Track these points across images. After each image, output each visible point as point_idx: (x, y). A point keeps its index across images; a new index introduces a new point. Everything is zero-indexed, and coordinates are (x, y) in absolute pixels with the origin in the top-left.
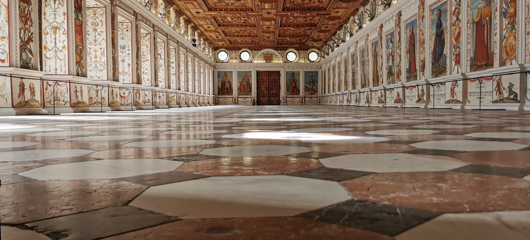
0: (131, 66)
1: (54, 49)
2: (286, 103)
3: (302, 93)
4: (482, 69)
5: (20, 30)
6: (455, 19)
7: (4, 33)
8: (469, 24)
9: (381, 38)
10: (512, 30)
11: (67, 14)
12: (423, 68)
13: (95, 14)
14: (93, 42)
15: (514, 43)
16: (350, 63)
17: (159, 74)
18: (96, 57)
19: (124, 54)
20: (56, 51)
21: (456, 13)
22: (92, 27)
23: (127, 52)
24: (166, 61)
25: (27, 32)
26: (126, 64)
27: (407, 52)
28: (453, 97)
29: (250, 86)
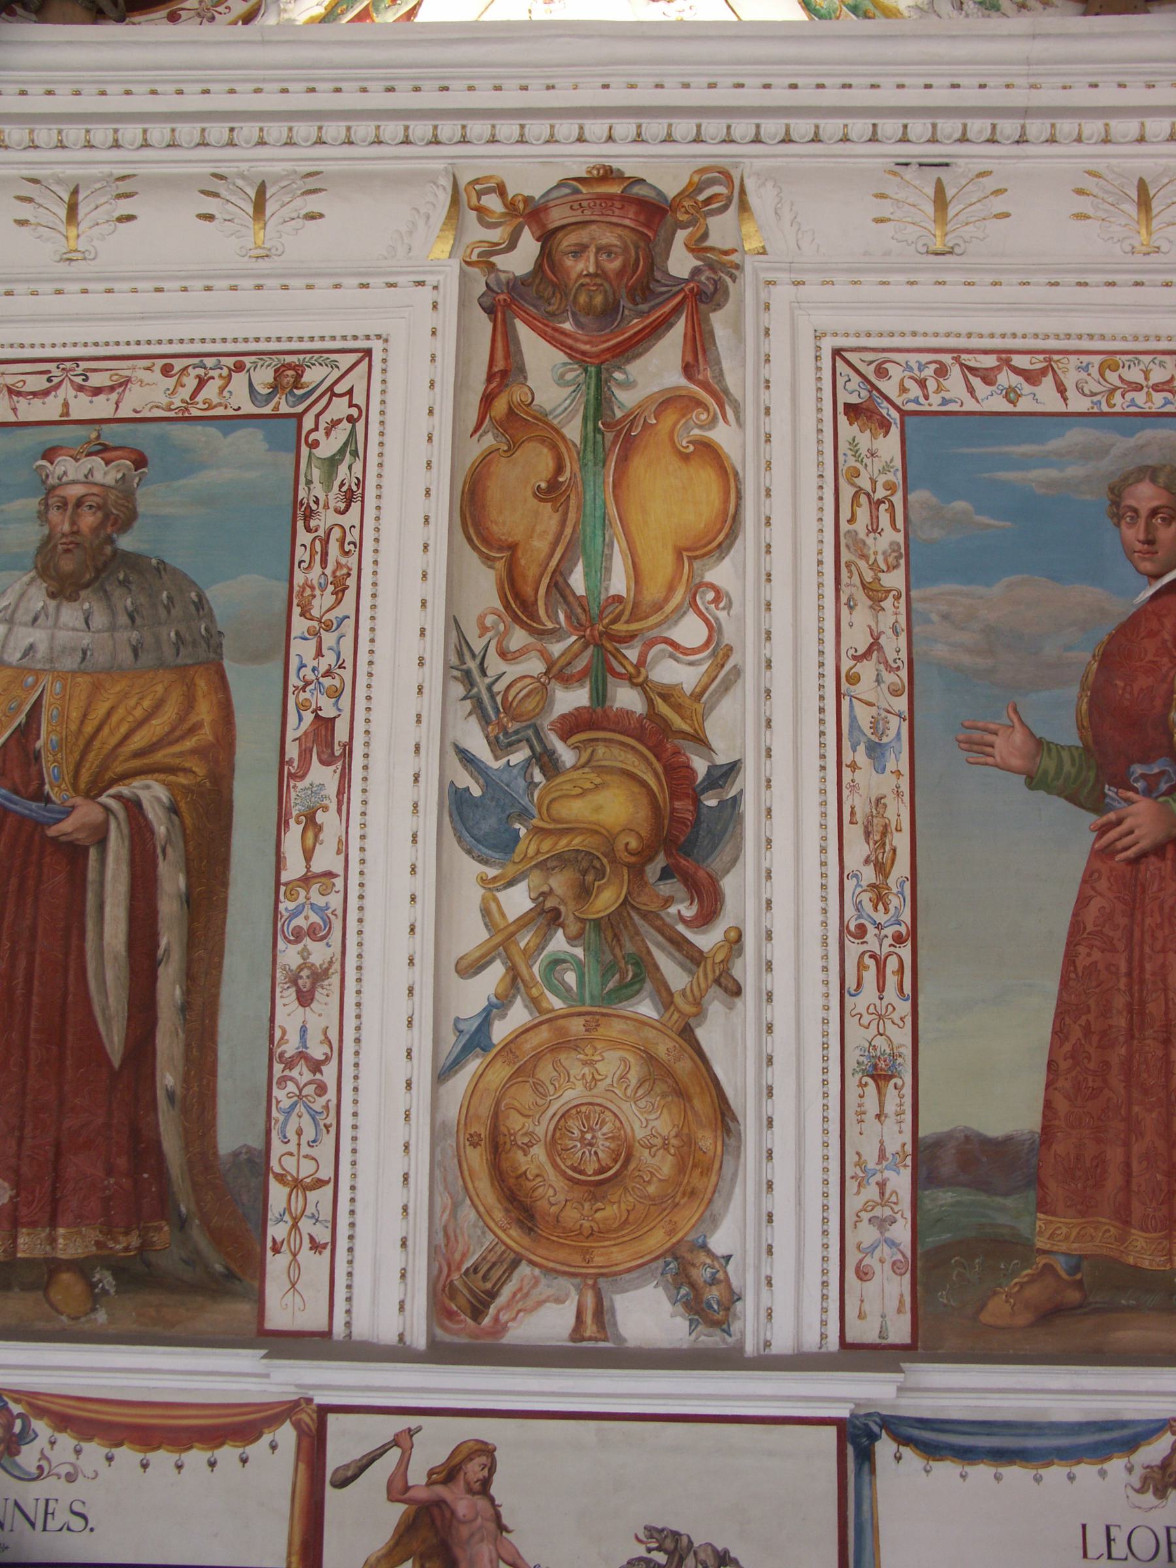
10: (627, 990)
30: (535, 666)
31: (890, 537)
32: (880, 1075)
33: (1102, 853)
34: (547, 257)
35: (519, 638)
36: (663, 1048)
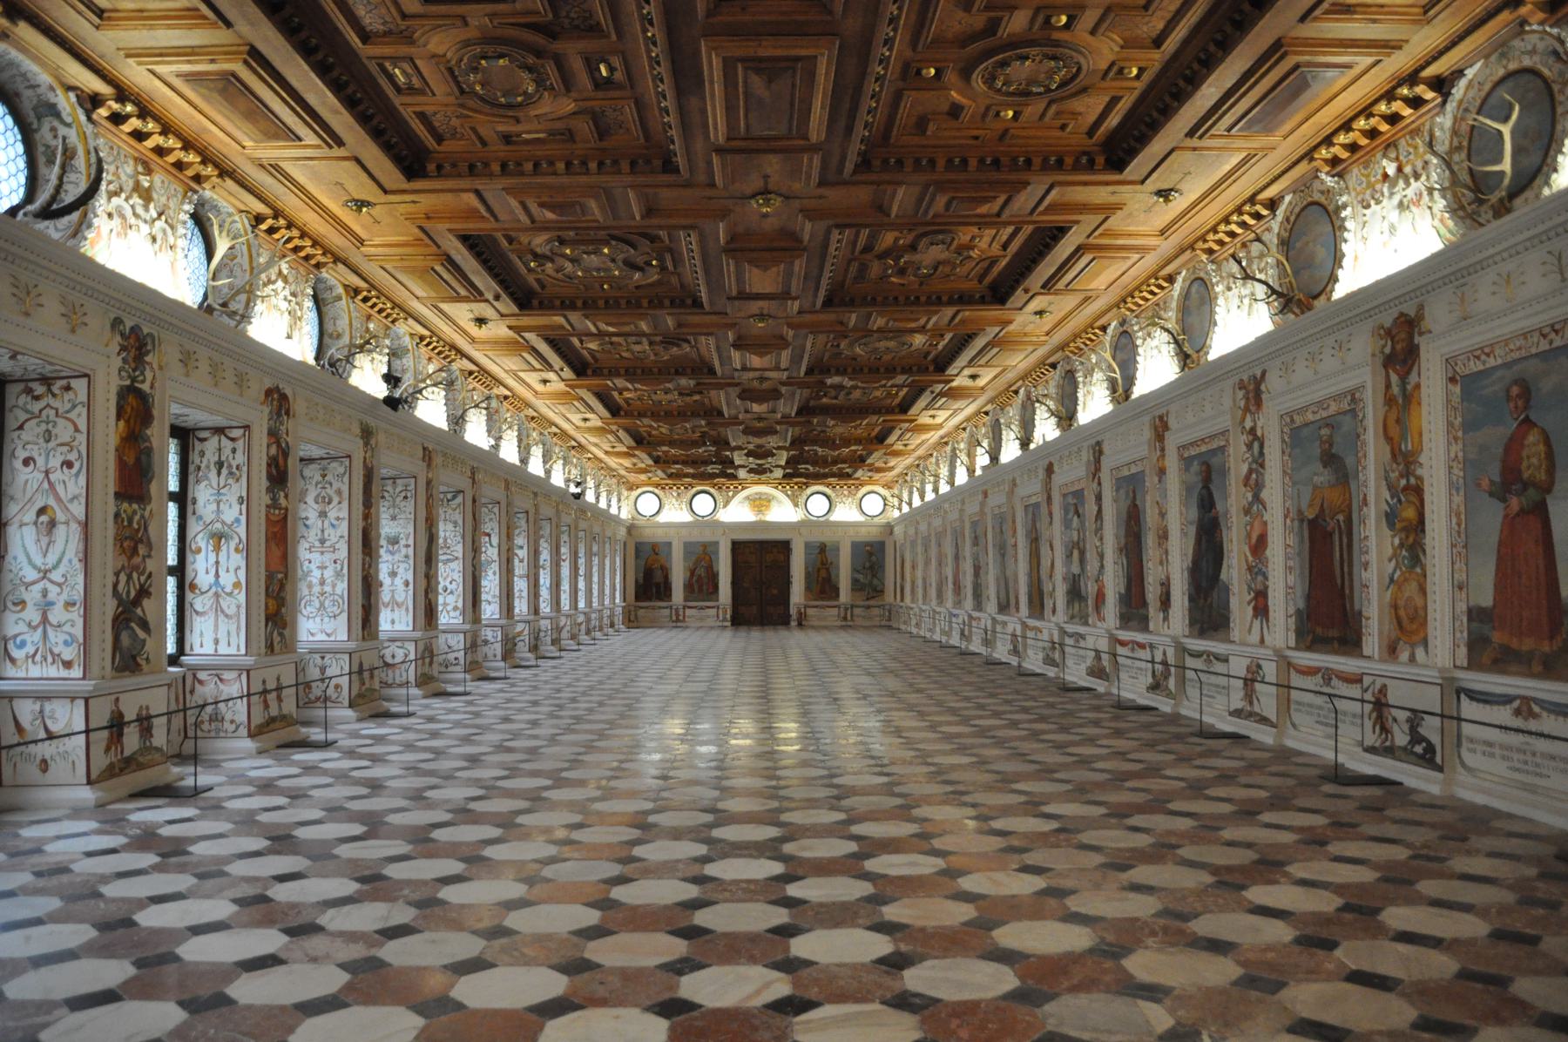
0: (411, 586)
1: (214, 589)
3: (845, 596)
5: (117, 574)
6: (1249, 496)
7: (74, 592)
9: (1049, 499)
10: (1413, 567)
11: (245, 501)
12: (1165, 603)
13: (324, 476)
14: (317, 544)
15: (1419, 602)
16: (968, 542)
17: (484, 583)
18: (322, 583)
19: (397, 557)
20: (217, 595)
21: (1252, 482)
22: (316, 506)
23: (404, 551)
24: (504, 548)
25: (135, 575)
26: (399, 581)
27: (1121, 550)
29: (713, 578)
30: (1397, 474)
32: (1461, 588)
33: (1506, 516)
34: (1393, 348)
35: (1395, 466)
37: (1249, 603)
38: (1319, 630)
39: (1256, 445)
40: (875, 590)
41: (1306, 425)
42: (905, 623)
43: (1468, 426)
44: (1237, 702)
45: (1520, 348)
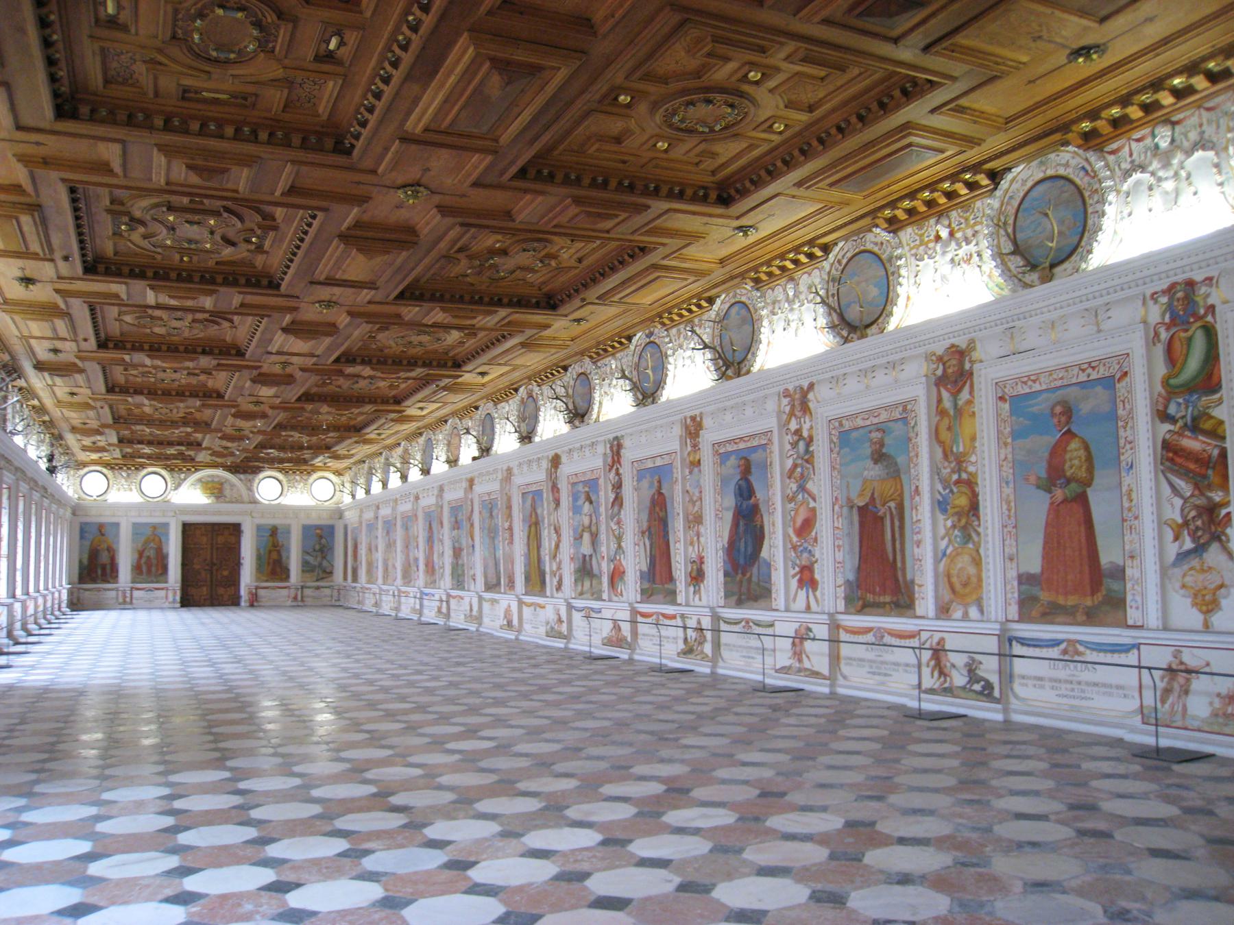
2: (254, 602)
4: (880, 611)
6: (794, 487)
8: (836, 507)
10: (966, 543)
12: (697, 577)
27: (643, 533)
28: (800, 661)
30: (949, 470)
31: (1008, 429)
32: (1011, 559)
33: (1052, 504)
34: (944, 370)
36: (974, 554)
37: (794, 576)
38: (870, 597)
39: (802, 445)
40: (324, 571)
41: (857, 429)
42: (359, 602)
43: (1015, 435)
44: (784, 659)
45: (1062, 378)
